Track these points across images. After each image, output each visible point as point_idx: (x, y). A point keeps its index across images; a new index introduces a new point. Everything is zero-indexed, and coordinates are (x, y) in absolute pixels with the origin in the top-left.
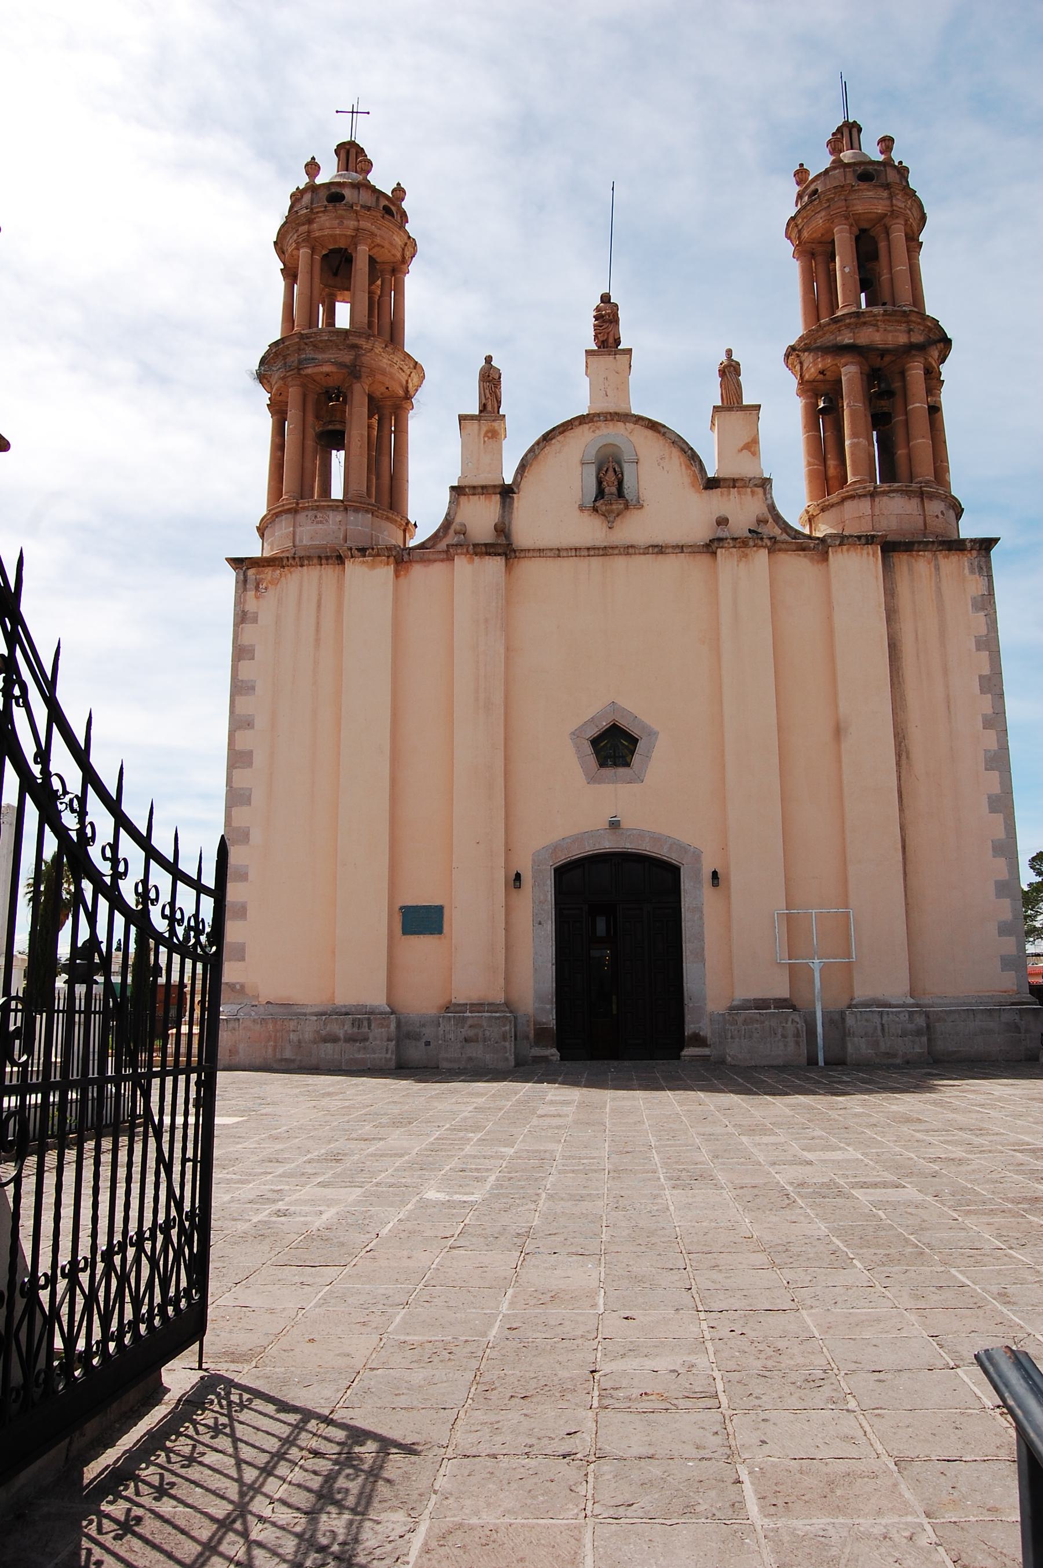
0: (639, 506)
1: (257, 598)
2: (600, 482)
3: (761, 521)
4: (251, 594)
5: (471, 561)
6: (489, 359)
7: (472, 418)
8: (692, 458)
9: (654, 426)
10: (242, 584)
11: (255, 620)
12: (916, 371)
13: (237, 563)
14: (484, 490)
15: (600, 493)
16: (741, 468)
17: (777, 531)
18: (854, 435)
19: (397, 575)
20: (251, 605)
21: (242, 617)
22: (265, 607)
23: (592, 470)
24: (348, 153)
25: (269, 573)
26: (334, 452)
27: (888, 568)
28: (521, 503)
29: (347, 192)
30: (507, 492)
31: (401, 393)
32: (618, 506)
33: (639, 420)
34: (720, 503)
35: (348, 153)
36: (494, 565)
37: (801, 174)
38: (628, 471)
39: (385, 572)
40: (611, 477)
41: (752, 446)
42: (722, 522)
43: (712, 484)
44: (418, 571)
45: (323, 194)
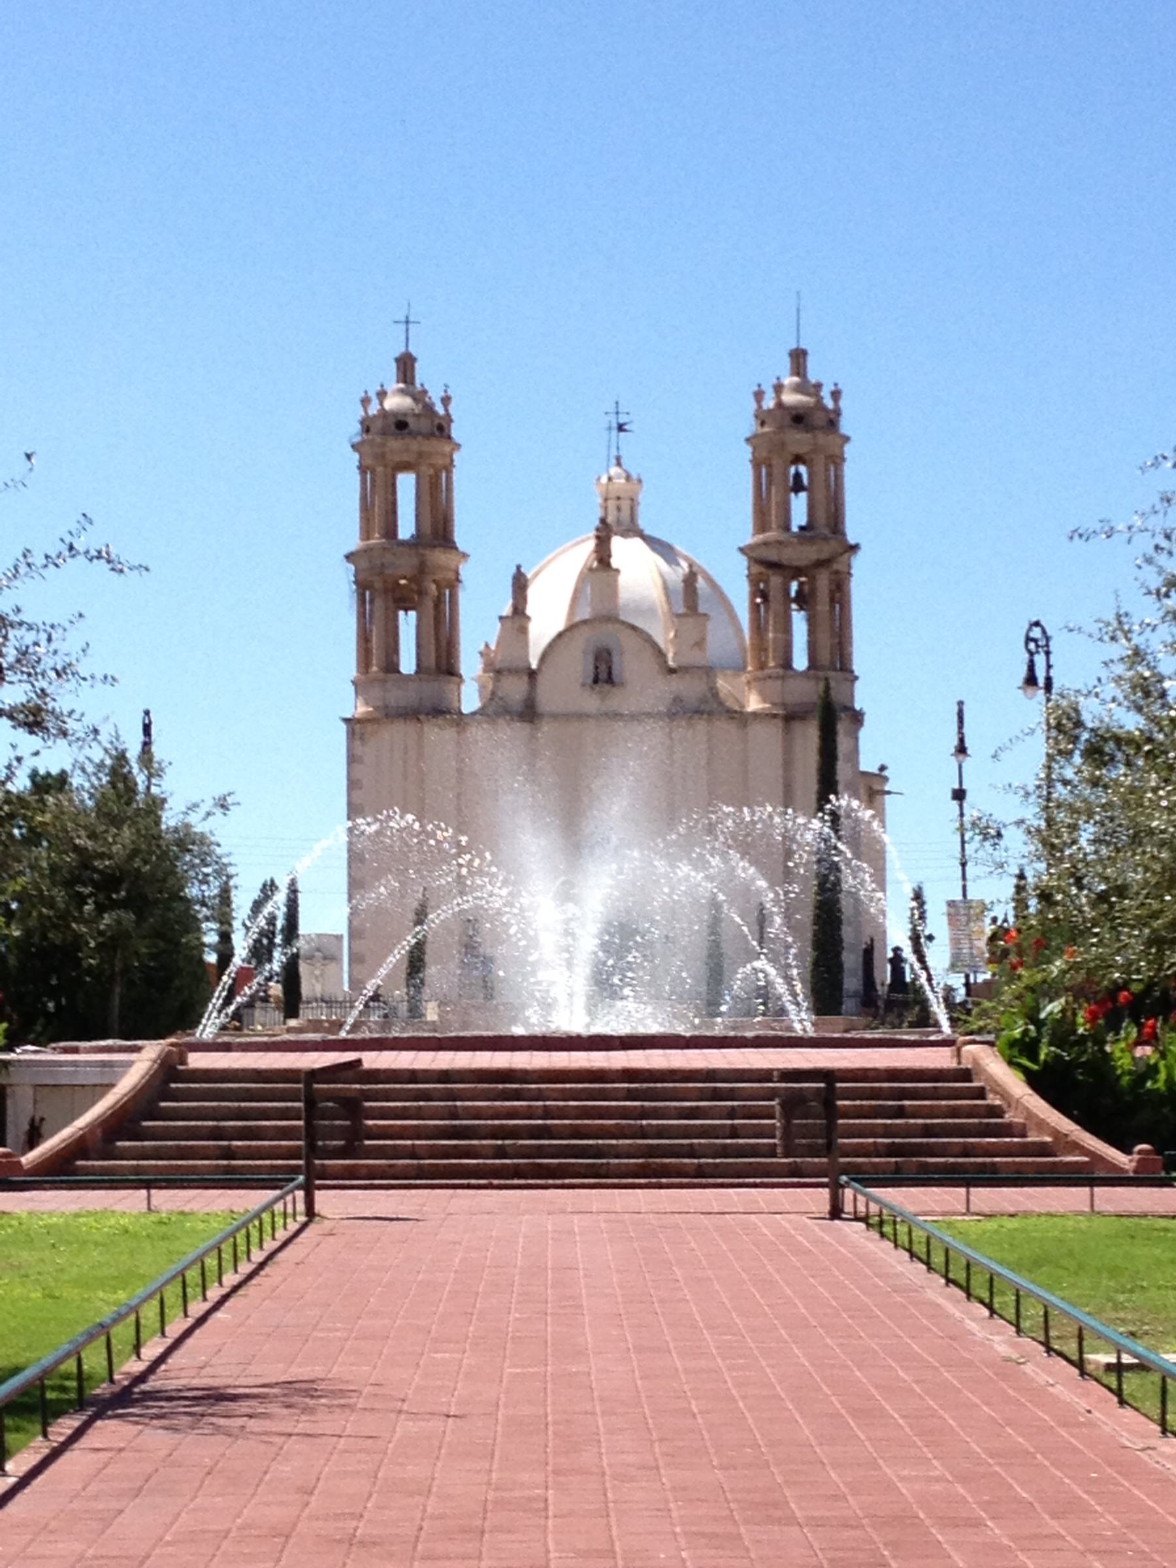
0: (622, 684)
1: (363, 745)
2: (597, 668)
3: (704, 700)
4: (358, 743)
5: (509, 725)
6: (519, 567)
7: (507, 617)
8: (660, 654)
9: (634, 628)
10: (351, 735)
11: (362, 762)
12: (823, 581)
13: (347, 721)
15: (596, 681)
16: (693, 657)
18: (775, 631)
19: (458, 733)
20: (359, 750)
21: (352, 759)
22: (367, 752)
23: (591, 659)
24: (405, 363)
25: (370, 727)
26: (401, 613)
27: (787, 731)
28: (543, 682)
29: (411, 421)
30: (532, 674)
31: (453, 577)
32: (607, 687)
33: (623, 623)
34: (677, 685)
35: (405, 363)
37: (759, 395)
38: (616, 659)
39: (450, 733)
40: (603, 668)
41: (700, 644)
43: (672, 671)
45: (391, 421)
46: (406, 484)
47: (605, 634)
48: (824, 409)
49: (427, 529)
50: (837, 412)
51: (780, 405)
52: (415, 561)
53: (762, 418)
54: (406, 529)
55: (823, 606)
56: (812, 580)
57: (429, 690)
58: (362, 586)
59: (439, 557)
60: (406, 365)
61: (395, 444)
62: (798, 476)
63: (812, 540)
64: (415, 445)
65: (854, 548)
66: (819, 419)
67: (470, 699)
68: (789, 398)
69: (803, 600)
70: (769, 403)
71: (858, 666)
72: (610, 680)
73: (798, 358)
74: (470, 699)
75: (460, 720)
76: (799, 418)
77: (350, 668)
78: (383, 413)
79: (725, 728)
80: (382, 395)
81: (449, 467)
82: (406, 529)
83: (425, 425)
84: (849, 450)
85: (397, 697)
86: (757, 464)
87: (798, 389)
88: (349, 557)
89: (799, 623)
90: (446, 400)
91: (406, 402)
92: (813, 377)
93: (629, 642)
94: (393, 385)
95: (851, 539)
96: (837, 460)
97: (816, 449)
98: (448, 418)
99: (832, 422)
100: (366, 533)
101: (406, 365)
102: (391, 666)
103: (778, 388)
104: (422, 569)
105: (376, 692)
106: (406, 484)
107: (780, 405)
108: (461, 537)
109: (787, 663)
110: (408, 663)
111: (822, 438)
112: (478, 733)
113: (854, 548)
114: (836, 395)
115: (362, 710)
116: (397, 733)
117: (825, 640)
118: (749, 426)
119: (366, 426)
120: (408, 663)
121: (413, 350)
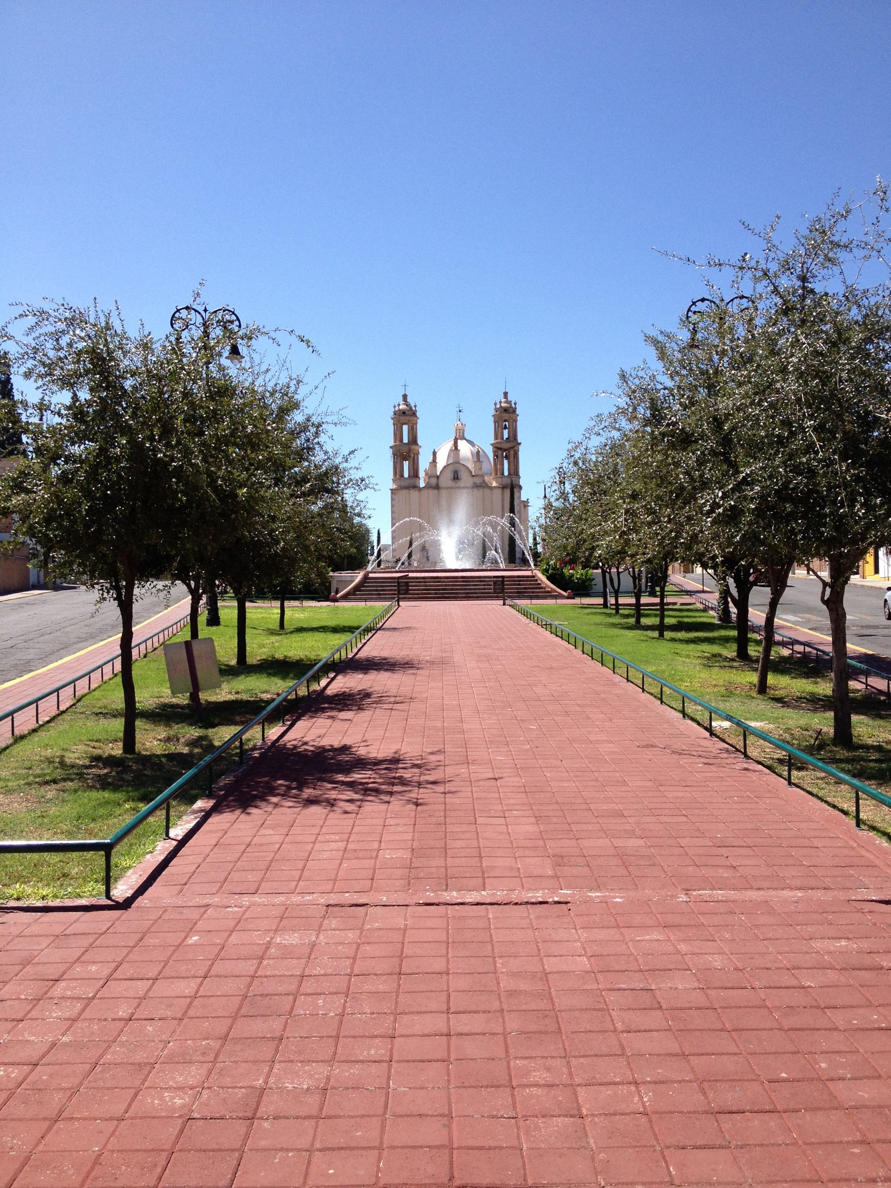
3: (481, 483)
12: (512, 452)
14: (434, 476)
16: (480, 473)
17: (484, 485)
21: (392, 499)
22: (396, 498)
27: (503, 491)
28: (440, 479)
30: (438, 477)
36: (436, 491)
37: (495, 404)
39: (417, 492)
41: (480, 469)
42: (475, 483)
43: (473, 476)
44: (423, 492)
46: (405, 428)
47: (457, 467)
48: (512, 407)
49: (411, 440)
50: (516, 408)
51: (501, 406)
52: (408, 448)
53: (496, 410)
54: (405, 440)
55: (512, 459)
56: (509, 452)
57: (412, 481)
58: (394, 454)
59: (414, 447)
60: (405, 397)
61: (402, 418)
62: (505, 425)
63: (509, 442)
64: (408, 418)
65: (520, 444)
66: (511, 410)
67: (422, 484)
68: (503, 405)
69: (507, 457)
70: (498, 406)
71: (521, 474)
72: (458, 479)
73: (506, 394)
74: (422, 484)
75: (420, 489)
76: (506, 410)
77: (392, 477)
78: (399, 410)
79: (487, 491)
80: (399, 405)
81: (416, 424)
82: (405, 440)
83: (410, 413)
84: (519, 418)
85: (404, 484)
86: (495, 422)
87: (506, 402)
88: (391, 447)
89: (506, 462)
90: (415, 406)
91: (405, 407)
92: (509, 399)
93: (462, 467)
94: (402, 402)
95: (519, 441)
96: (516, 421)
97: (510, 418)
98: (416, 411)
99: (514, 411)
100: (395, 442)
101: (405, 397)
102: (402, 476)
103: (500, 402)
104: (410, 450)
105: (398, 482)
106: (405, 428)
107: (501, 406)
108: (419, 442)
109: (503, 474)
110: (406, 475)
111: (512, 415)
112: (425, 492)
113: (520, 444)
114: (515, 404)
115: (395, 487)
116: (405, 492)
117: (512, 467)
118: (493, 412)
119: (395, 413)
120: (406, 475)
121: (407, 394)
